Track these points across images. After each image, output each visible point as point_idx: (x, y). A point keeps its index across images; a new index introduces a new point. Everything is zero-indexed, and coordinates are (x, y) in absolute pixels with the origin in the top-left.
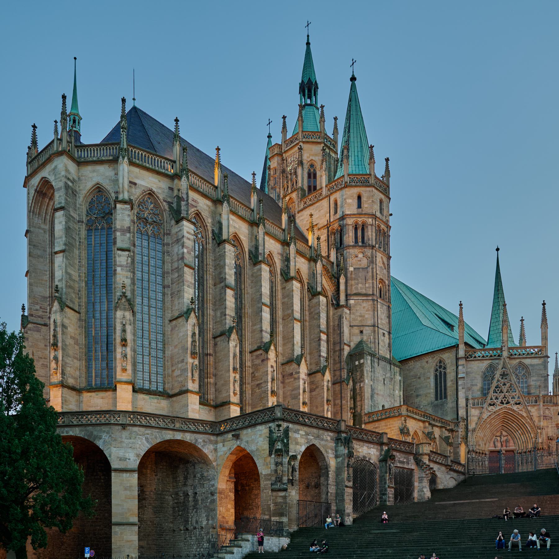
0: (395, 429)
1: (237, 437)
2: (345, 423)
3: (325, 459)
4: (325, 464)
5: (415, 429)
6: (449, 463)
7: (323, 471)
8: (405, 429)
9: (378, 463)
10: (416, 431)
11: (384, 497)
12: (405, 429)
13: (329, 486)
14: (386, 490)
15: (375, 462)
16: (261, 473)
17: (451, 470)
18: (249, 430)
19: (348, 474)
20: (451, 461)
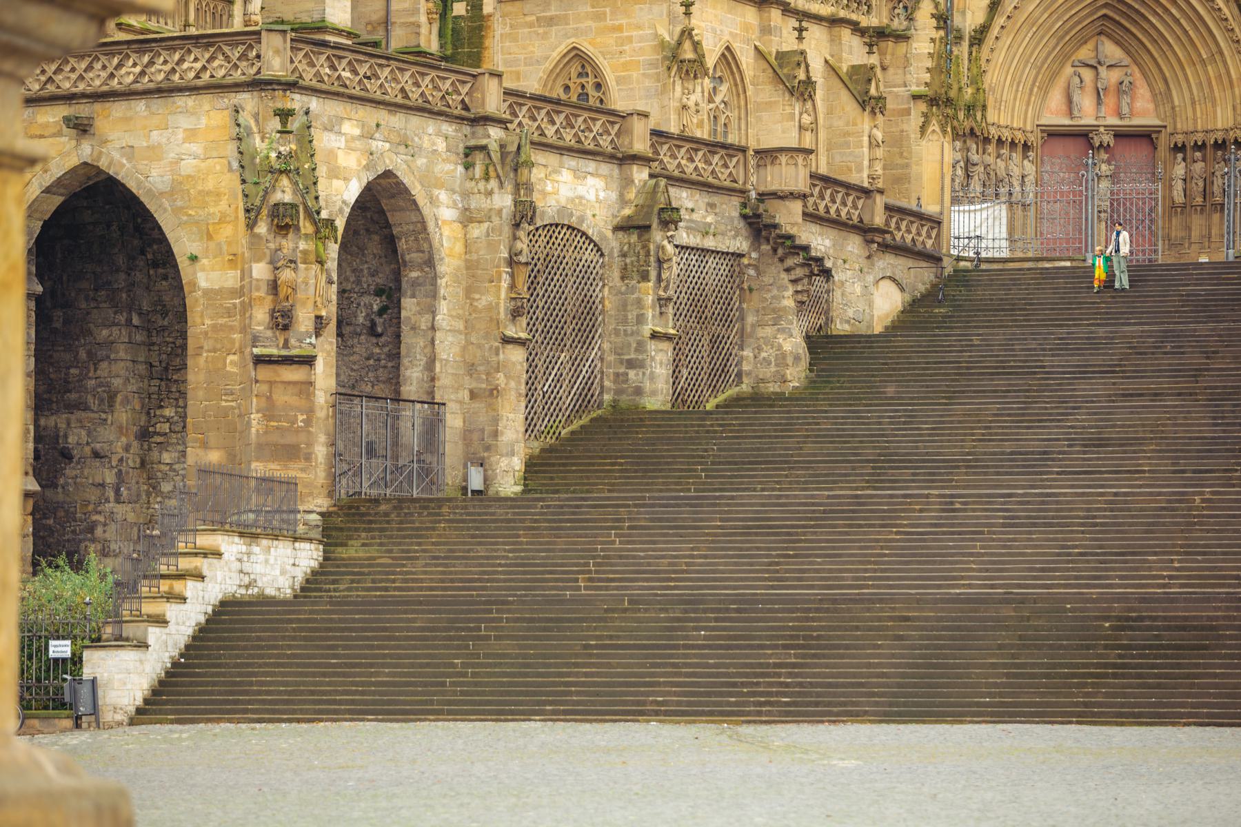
0: (641, 39)
1: (82, 128)
2: (500, 83)
3: (425, 228)
4: (426, 246)
5: (726, 37)
6: (879, 220)
7: (414, 274)
8: (687, 45)
9: (609, 234)
10: (728, 48)
11: (632, 374)
12: (687, 45)
13: (438, 334)
14: (640, 347)
15: (600, 232)
16: (194, 284)
17: (886, 247)
18: (140, 106)
19: (512, 286)
20: (889, 208)
